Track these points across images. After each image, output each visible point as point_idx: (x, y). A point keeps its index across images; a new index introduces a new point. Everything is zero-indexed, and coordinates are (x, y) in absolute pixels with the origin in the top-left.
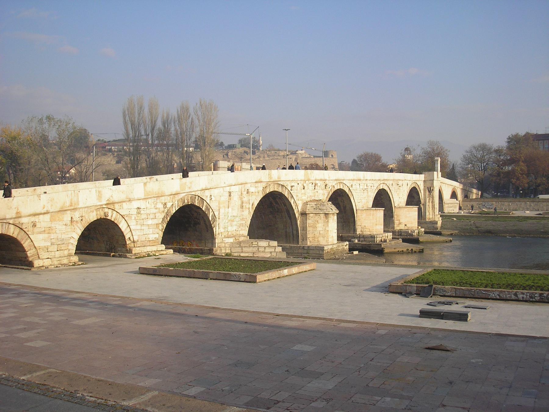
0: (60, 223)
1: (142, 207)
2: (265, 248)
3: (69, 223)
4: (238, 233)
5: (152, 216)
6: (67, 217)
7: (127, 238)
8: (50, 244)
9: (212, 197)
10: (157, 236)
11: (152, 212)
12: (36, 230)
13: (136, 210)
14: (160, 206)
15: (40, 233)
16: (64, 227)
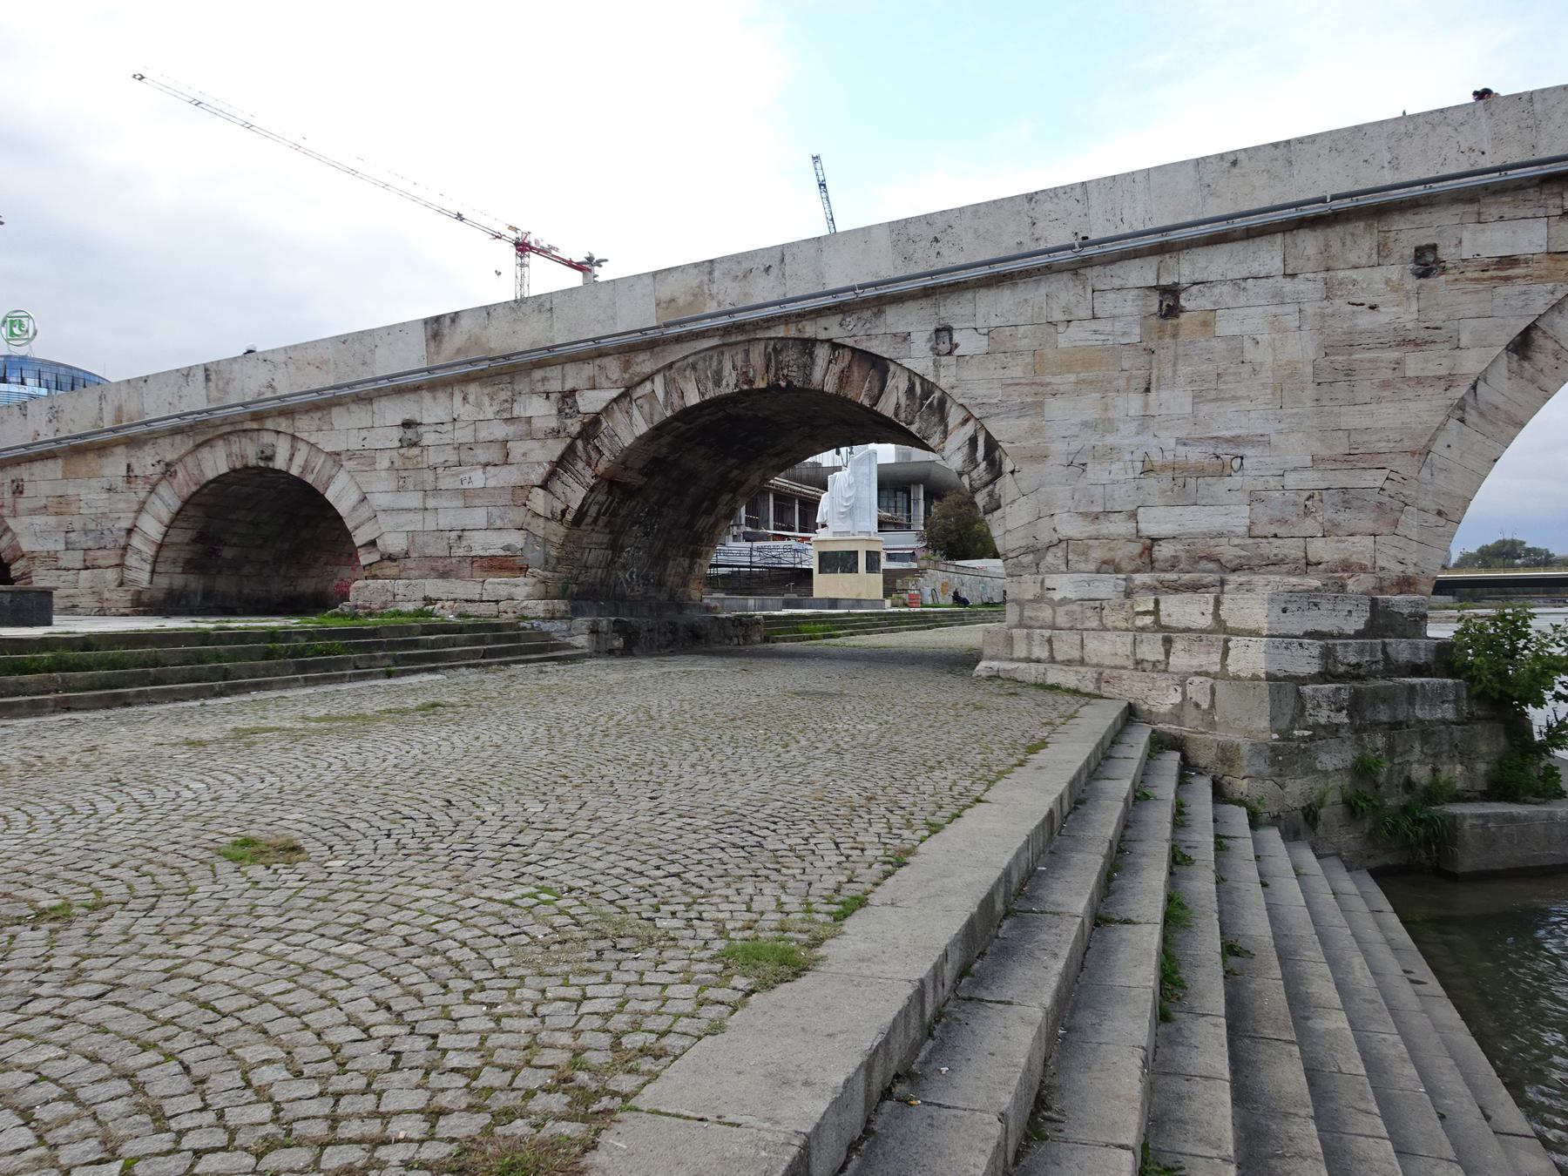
0: (94, 483)
1: (427, 419)
2: (1168, 642)
3: (120, 484)
4: (1269, 549)
5: (482, 455)
6: (114, 467)
7: (359, 538)
8: (61, 546)
9: (957, 337)
10: (516, 539)
11: (483, 435)
12: (23, 503)
13: (397, 433)
14: (540, 410)
15: (33, 512)
16: (105, 496)
